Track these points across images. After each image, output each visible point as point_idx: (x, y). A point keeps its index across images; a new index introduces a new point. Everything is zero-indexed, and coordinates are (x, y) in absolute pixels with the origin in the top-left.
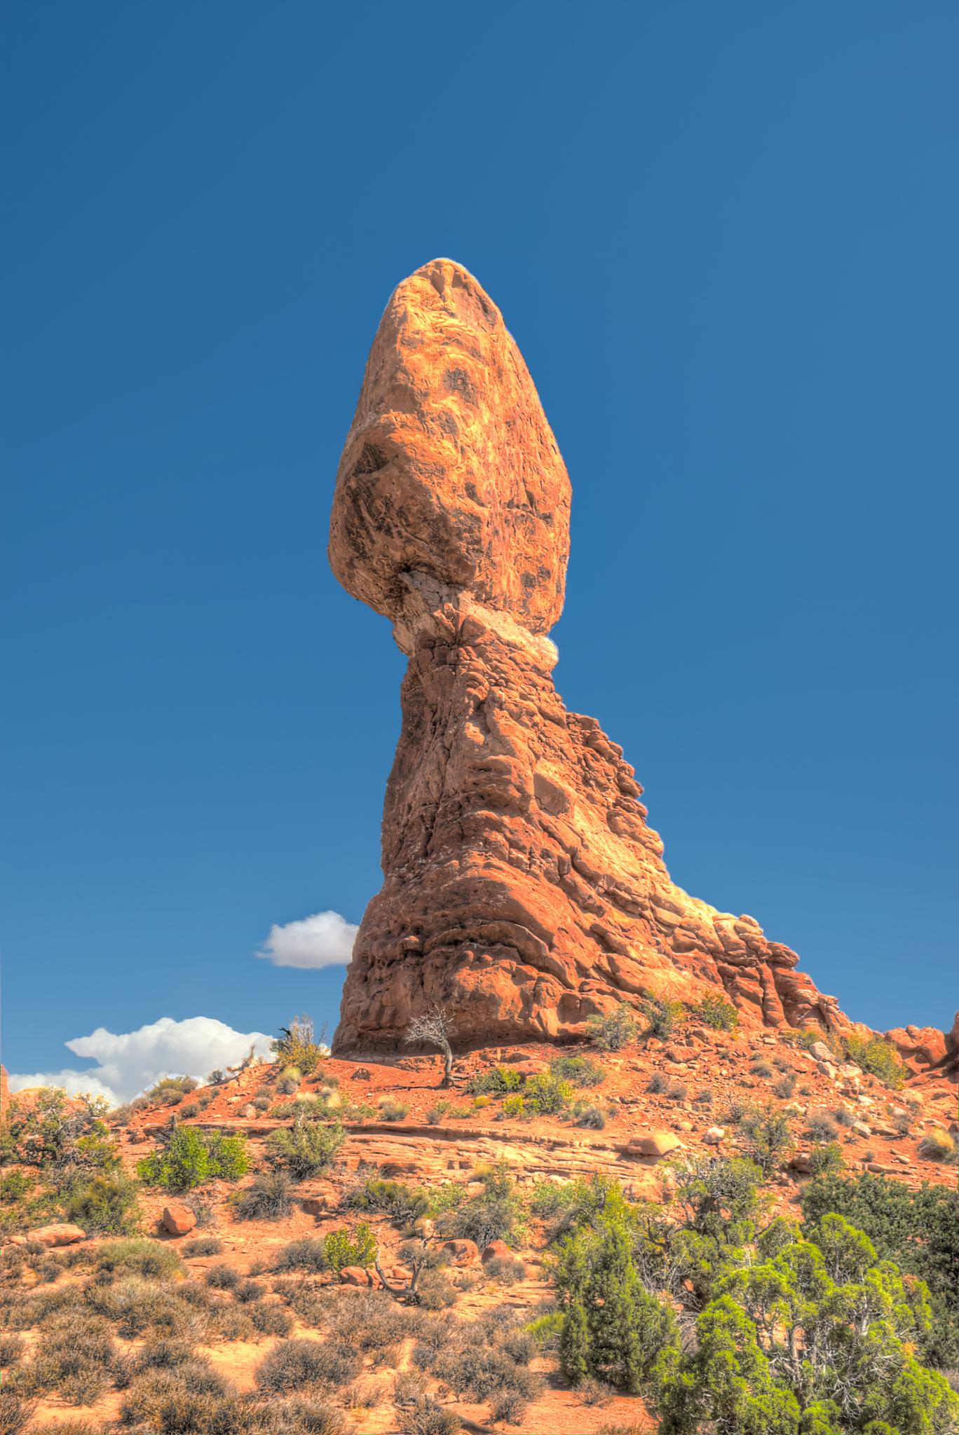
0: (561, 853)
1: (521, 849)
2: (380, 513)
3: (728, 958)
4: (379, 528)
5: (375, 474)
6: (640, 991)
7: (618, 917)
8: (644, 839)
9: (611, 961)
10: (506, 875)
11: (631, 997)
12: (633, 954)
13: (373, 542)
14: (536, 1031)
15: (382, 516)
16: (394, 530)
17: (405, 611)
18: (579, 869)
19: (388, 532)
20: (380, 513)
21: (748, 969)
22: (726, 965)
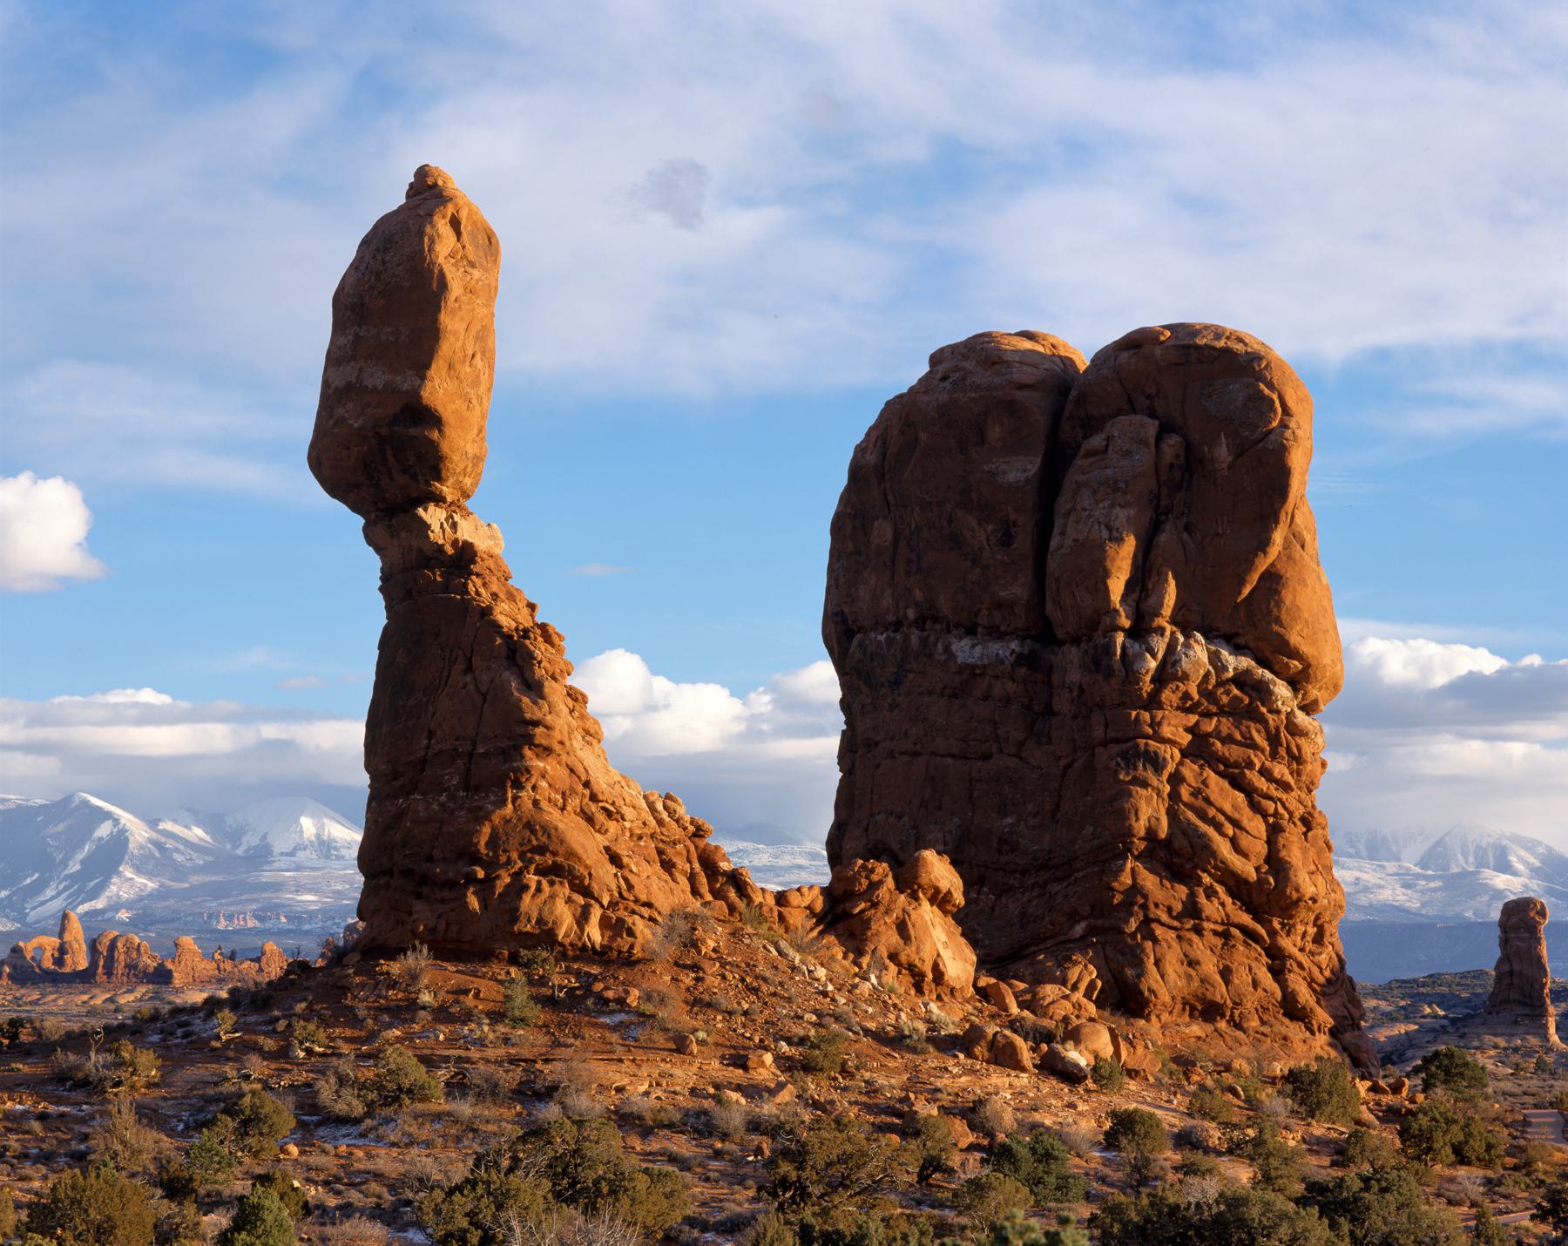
0: (580, 788)
1: (557, 791)
2: (409, 460)
3: (663, 837)
4: (404, 471)
5: (413, 431)
6: (649, 905)
7: (612, 827)
8: (592, 731)
9: (626, 880)
10: (552, 815)
11: (646, 912)
12: (634, 869)
13: (392, 479)
14: (584, 945)
15: (411, 463)
16: (420, 478)
17: (393, 522)
18: (594, 798)
19: (414, 477)
20: (409, 460)
21: (680, 847)
22: (661, 845)
